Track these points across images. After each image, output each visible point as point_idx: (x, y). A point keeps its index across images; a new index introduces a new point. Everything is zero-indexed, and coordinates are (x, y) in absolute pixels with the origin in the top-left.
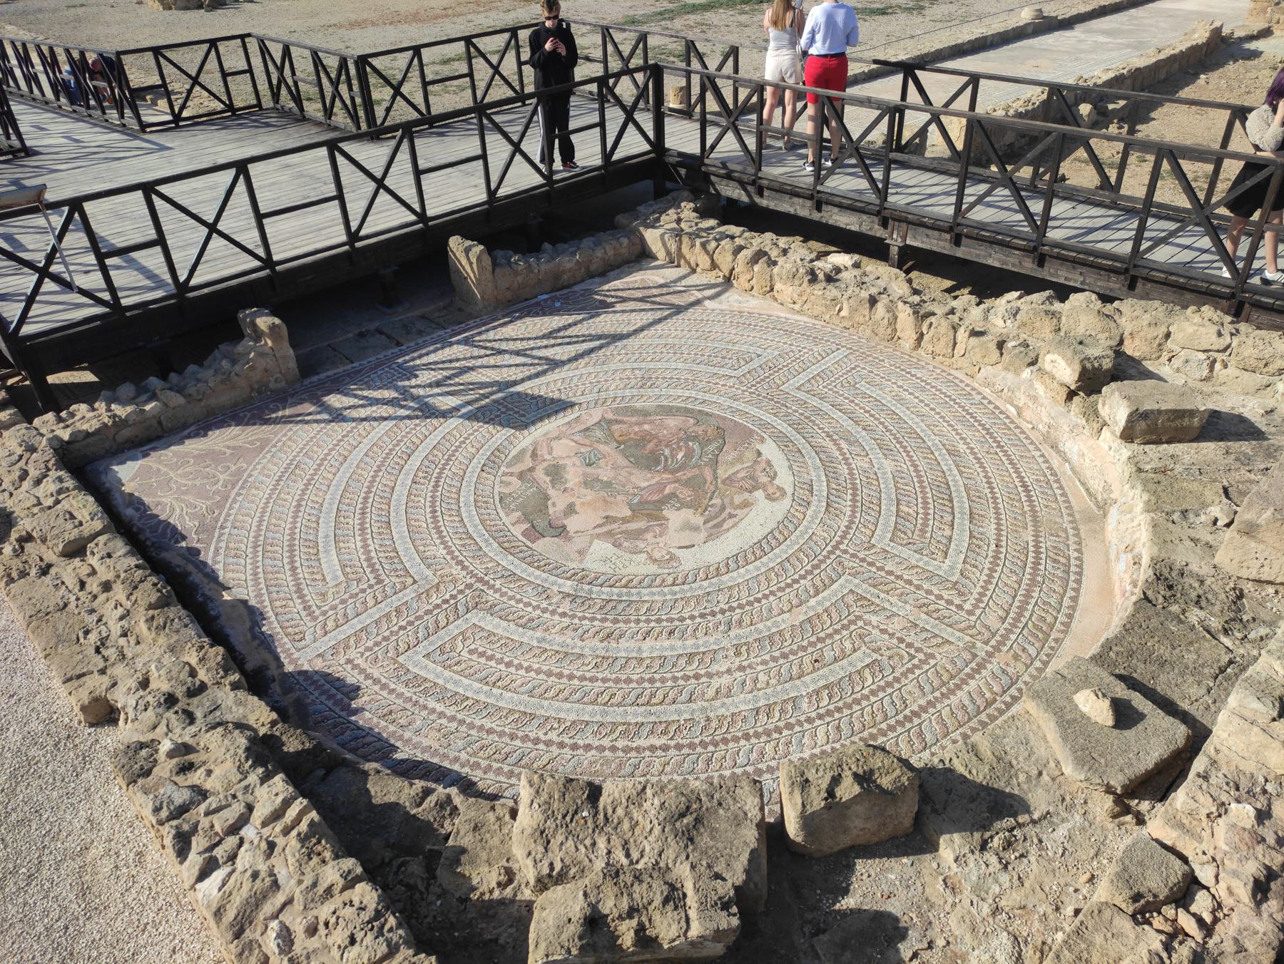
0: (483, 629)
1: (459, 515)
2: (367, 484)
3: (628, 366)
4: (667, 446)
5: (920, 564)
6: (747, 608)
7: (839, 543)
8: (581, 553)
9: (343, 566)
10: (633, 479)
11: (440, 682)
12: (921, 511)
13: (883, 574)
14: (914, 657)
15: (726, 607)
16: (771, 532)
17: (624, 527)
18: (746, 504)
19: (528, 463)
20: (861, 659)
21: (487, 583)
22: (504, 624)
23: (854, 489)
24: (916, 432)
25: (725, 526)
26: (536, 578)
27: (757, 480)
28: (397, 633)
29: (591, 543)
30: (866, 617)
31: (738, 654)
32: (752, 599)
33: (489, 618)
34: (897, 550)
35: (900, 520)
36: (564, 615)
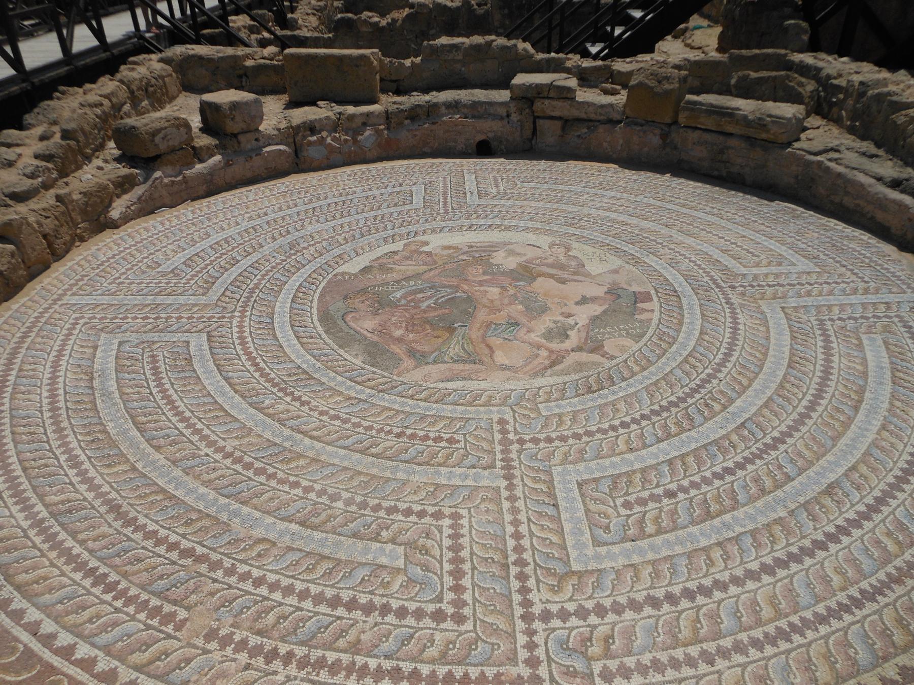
2: (804, 429)
9: (860, 346)
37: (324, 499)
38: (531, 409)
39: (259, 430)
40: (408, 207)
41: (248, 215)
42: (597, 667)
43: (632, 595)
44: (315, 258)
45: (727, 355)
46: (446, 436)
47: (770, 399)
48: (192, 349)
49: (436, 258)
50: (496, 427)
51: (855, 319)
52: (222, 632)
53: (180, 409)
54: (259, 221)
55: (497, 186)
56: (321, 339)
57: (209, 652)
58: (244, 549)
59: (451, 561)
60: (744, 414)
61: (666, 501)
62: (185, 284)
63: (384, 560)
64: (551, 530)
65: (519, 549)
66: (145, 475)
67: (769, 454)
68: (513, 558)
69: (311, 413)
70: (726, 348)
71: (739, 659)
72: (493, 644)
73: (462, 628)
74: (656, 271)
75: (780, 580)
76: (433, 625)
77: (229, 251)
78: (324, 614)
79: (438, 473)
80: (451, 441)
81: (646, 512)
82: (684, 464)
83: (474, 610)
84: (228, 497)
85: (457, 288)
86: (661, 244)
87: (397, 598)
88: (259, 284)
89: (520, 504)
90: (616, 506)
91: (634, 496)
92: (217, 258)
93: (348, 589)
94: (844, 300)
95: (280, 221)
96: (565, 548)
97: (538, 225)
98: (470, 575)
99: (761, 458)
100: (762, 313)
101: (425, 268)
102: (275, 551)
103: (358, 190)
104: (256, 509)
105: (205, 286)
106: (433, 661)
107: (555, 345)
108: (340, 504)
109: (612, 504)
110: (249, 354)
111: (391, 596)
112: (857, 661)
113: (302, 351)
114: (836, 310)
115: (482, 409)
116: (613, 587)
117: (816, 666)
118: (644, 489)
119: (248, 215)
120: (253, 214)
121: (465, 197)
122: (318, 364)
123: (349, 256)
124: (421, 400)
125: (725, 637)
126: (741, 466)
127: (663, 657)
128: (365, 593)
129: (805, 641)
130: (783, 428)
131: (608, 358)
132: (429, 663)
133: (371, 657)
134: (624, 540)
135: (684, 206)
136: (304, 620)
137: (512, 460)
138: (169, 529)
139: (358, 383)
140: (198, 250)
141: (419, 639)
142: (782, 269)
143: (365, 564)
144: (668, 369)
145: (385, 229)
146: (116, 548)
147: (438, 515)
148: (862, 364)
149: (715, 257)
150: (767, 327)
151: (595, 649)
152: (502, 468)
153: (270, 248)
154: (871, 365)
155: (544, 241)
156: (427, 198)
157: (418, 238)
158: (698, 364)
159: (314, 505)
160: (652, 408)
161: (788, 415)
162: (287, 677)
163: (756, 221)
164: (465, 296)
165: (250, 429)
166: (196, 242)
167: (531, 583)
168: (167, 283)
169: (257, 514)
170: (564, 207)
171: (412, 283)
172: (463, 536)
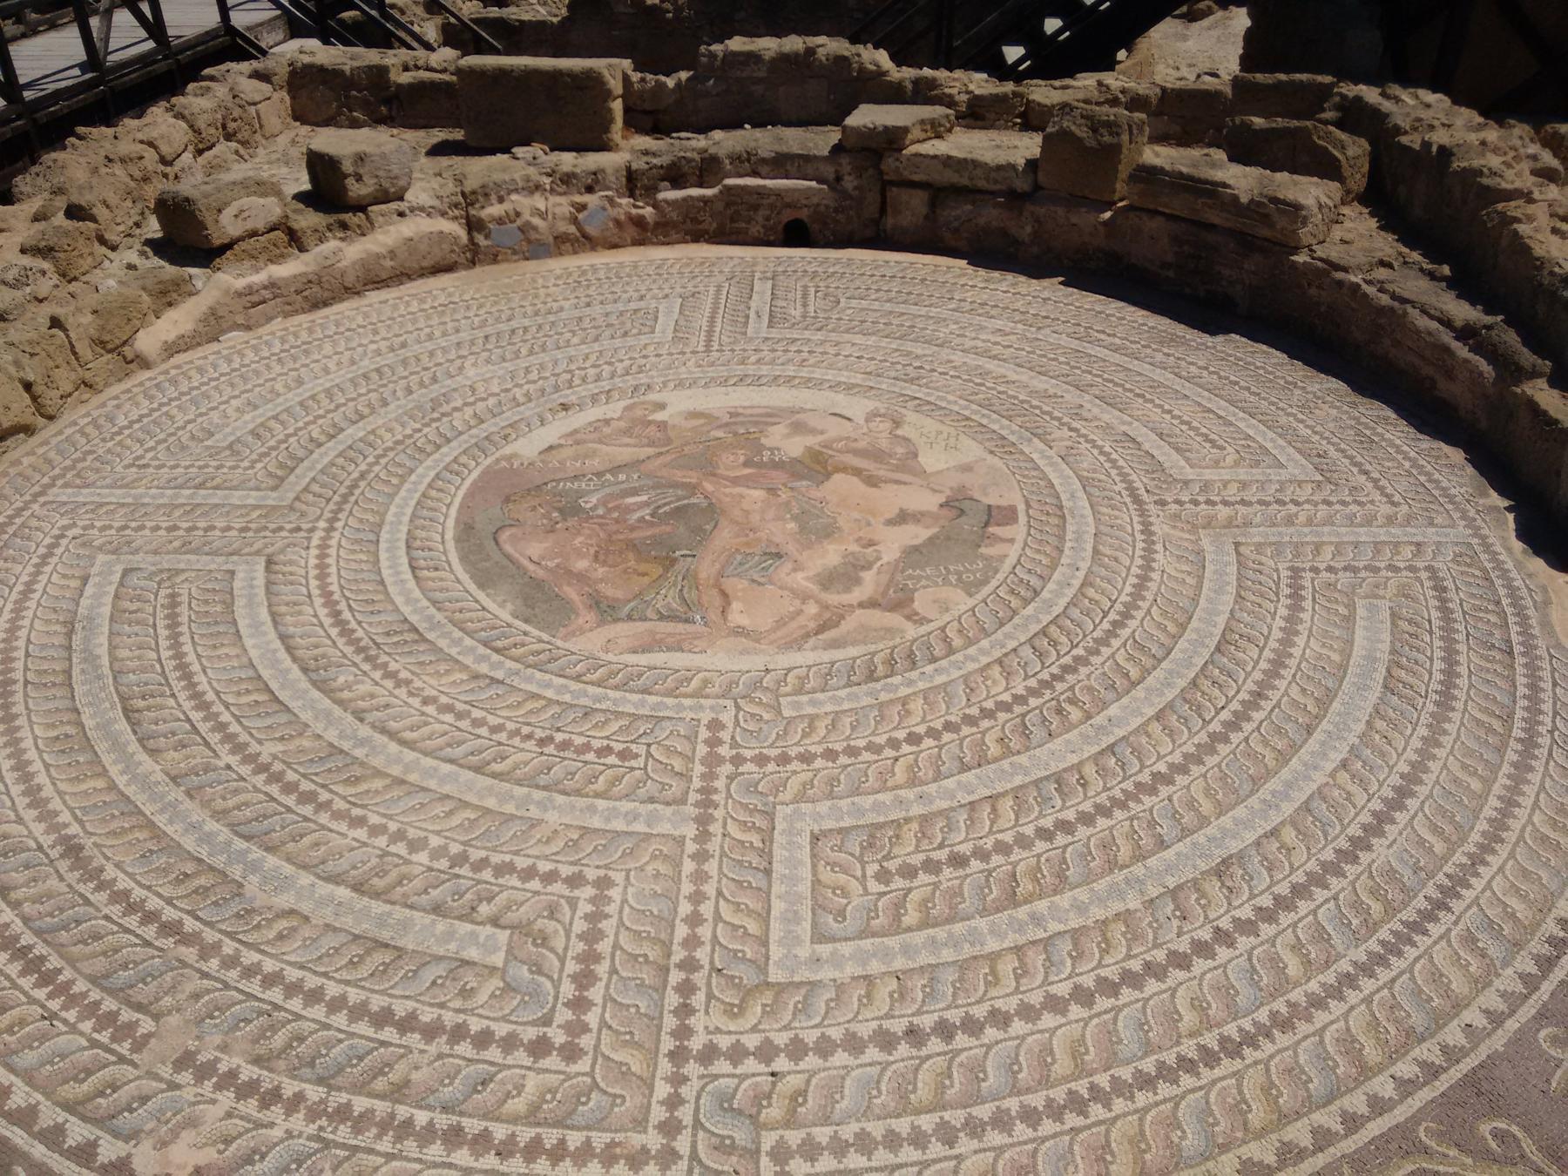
9: (1350, 619)
28: (1308, 501)
37: (400, 848)
38: (768, 705)
39: (319, 728)
40: (644, 339)
41: (374, 346)
42: (768, 1140)
43: (853, 1027)
44: (471, 428)
46: (618, 747)
47: (1170, 706)
48: (237, 584)
49: (672, 434)
50: (704, 734)
51: (1355, 570)
52: (202, 1058)
53: (199, 688)
54: (390, 358)
55: (805, 305)
56: (452, 571)
57: (178, 1087)
58: (258, 927)
59: (579, 959)
60: (1116, 730)
61: (947, 872)
62: (246, 469)
63: (472, 953)
64: (750, 912)
65: (692, 942)
66: (128, 798)
67: (1139, 801)
68: (679, 954)
69: (410, 700)
70: (1119, 613)
71: (995, 1138)
72: (615, 1096)
73: (573, 1068)
74: (1037, 468)
75: (1098, 1015)
76: (528, 1062)
77: (328, 412)
78: (362, 1037)
79: (592, 809)
80: (624, 755)
81: (910, 890)
82: (994, 810)
83: (599, 1039)
84: (248, 838)
85: (693, 489)
86: (1059, 419)
87: (480, 1016)
88: (368, 471)
89: (711, 867)
90: (864, 876)
91: (898, 861)
92: (307, 424)
93: (407, 997)
94: (1346, 534)
95: (425, 359)
96: (765, 943)
97: (858, 379)
98: (603, 983)
99: (1123, 805)
100: (1200, 553)
101: (651, 451)
102: (306, 932)
103: (566, 304)
104: (289, 860)
105: (279, 473)
106: (514, 1120)
107: (833, 598)
108: (422, 857)
109: (859, 873)
110: (327, 595)
111: (472, 1012)
112: (1180, 1150)
113: (417, 593)
114: (1328, 552)
115: (687, 702)
116: (827, 1013)
117: (1113, 1155)
118: (917, 850)
119: (374, 346)
120: (383, 345)
121: (747, 323)
122: (439, 616)
123: (528, 425)
124: (592, 683)
125: (983, 1103)
126: (1087, 819)
127: (876, 1129)
128: (431, 1005)
129: (1109, 1115)
130: (1177, 758)
131: (915, 622)
132: (507, 1122)
133: (421, 1108)
134: (864, 934)
135: (1116, 349)
136: (329, 1044)
137: (716, 791)
138: (149, 888)
139: (497, 651)
140: (279, 409)
141: (503, 1082)
142: (1257, 473)
143: (441, 958)
144: (1012, 644)
145: (598, 378)
146: (64, 916)
147: (575, 881)
148: (1342, 652)
149: (1146, 446)
150: (1201, 578)
151: (774, 1112)
152: (697, 804)
153: (399, 407)
154: (1358, 652)
155: (858, 407)
156: (682, 323)
157: (653, 397)
158: (1064, 639)
159: (381, 857)
160: (967, 711)
161: (1192, 734)
162: (287, 1131)
163: (1236, 383)
164: (705, 504)
165: (307, 725)
166: (279, 395)
167: (698, 1000)
168: (218, 468)
169: (289, 869)
170: (909, 346)
171: (622, 477)
172: (607, 916)
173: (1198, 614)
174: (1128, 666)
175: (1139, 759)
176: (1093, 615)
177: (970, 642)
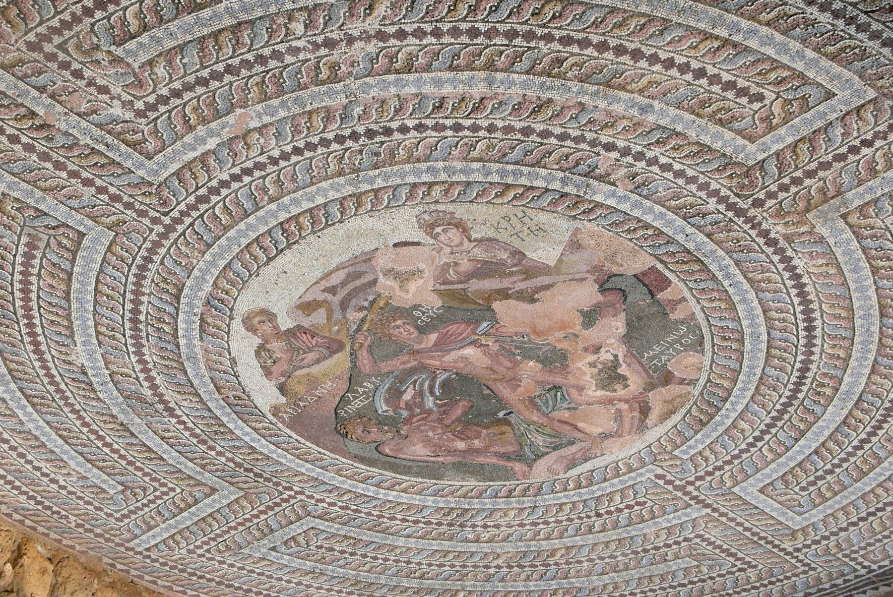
0: (739, 132)
1: (768, 319)
3: (486, 548)
4: (429, 412)
5: (39, 194)
6: (315, 140)
7: (164, 236)
8: (575, 245)
10: (486, 361)
11: (810, 54)
12: (33, 279)
13: (99, 182)
14: (60, 47)
15: (349, 143)
16: (270, 259)
17: (505, 283)
18: (307, 307)
19: (657, 399)
20: (138, 51)
21: (730, 207)
22: (706, 139)
23: (135, 321)
24: (33, 405)
25: (341, 275)
26: (651, 210)
27: (286, 347)
28: (876, 136)
29: (560, 261)
30: (129, 115)
31: (334, 67)
32: (308, 154)
33: (729, 151)
34: (75, 220)
35: (66, 265)
36: (609, 147)
45: (810, 329)
82: (827, 449)
100: (821, 240)
144: (759, 371)
173: (855, 295)
174: (836, 351)
175: (880, 398)
176: (789, 330)
177: (735, 382)
